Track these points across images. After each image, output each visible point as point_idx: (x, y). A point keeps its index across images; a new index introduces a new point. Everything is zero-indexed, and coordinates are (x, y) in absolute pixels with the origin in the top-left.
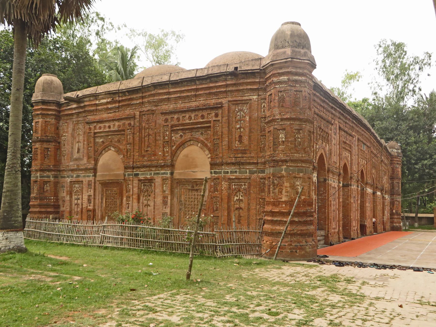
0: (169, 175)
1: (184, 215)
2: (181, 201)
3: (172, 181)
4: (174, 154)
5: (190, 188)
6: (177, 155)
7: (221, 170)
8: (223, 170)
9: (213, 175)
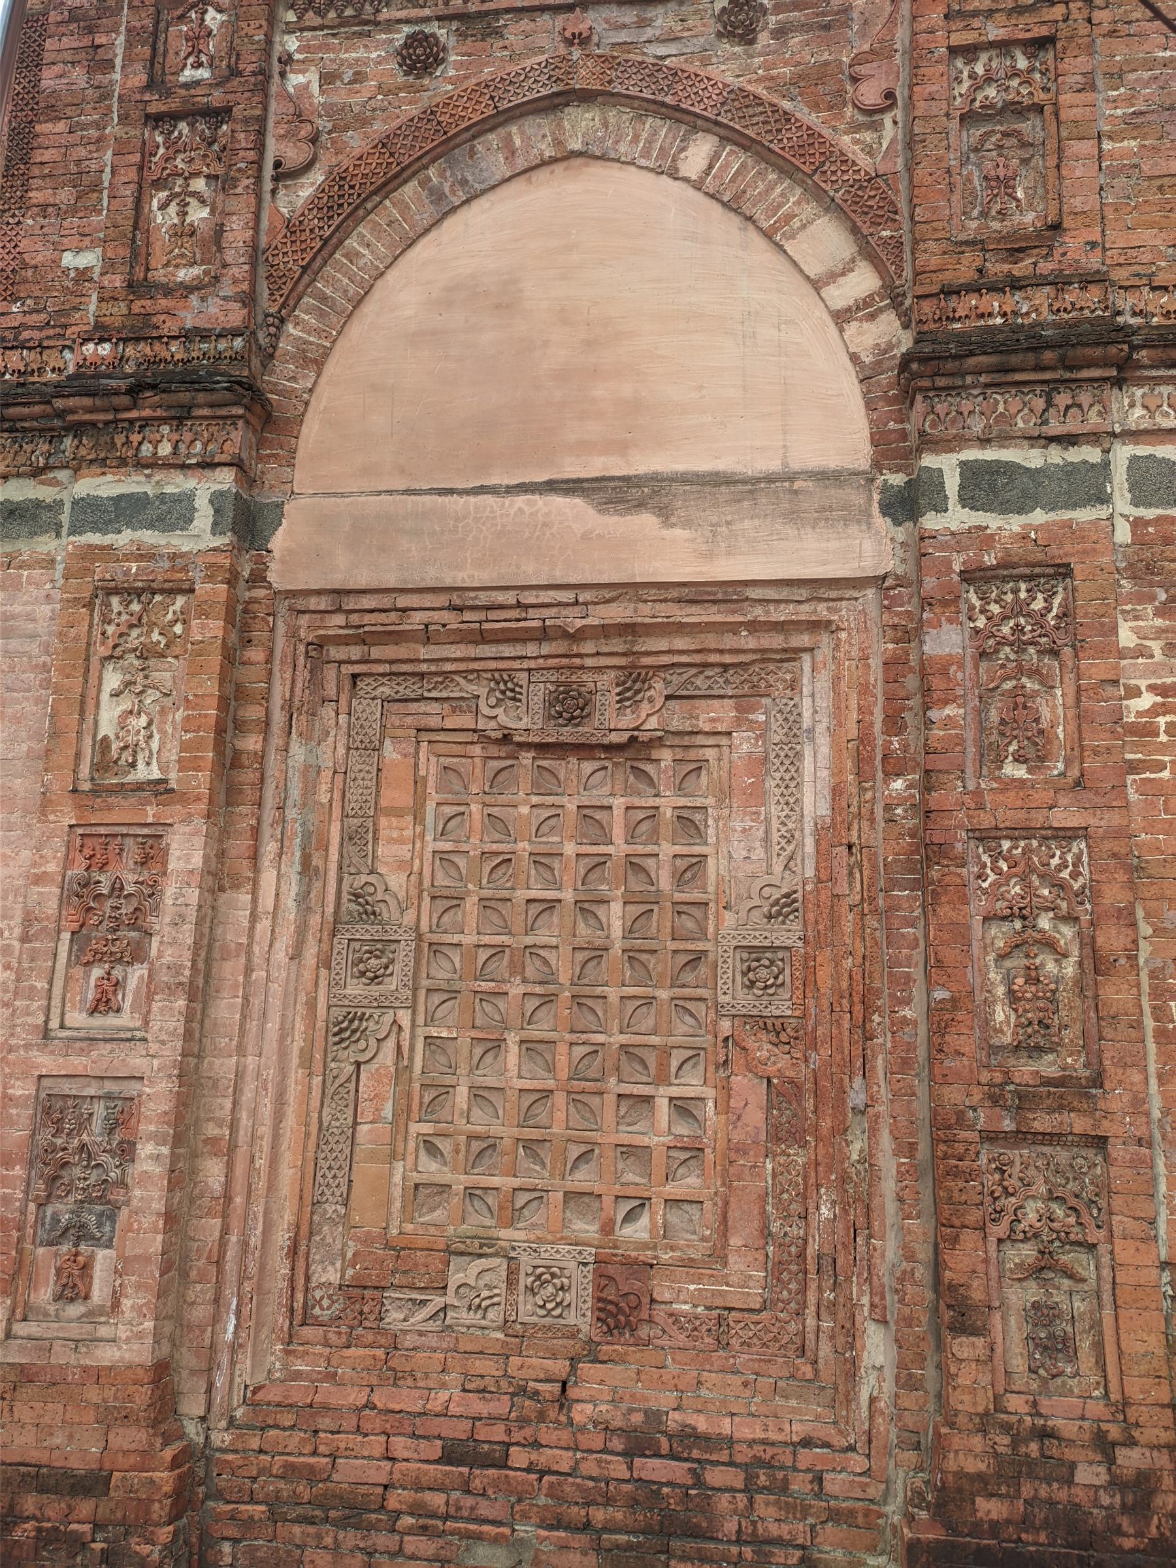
0: (202, 536)
1: (403, 1114)
2: (365, 907)
3: (242, 621)
4: (297, 269)
5: (525, 720)
6: (335, 281)
7: (1091, 454)
8: (1122, 453)
9: (956, 518)
